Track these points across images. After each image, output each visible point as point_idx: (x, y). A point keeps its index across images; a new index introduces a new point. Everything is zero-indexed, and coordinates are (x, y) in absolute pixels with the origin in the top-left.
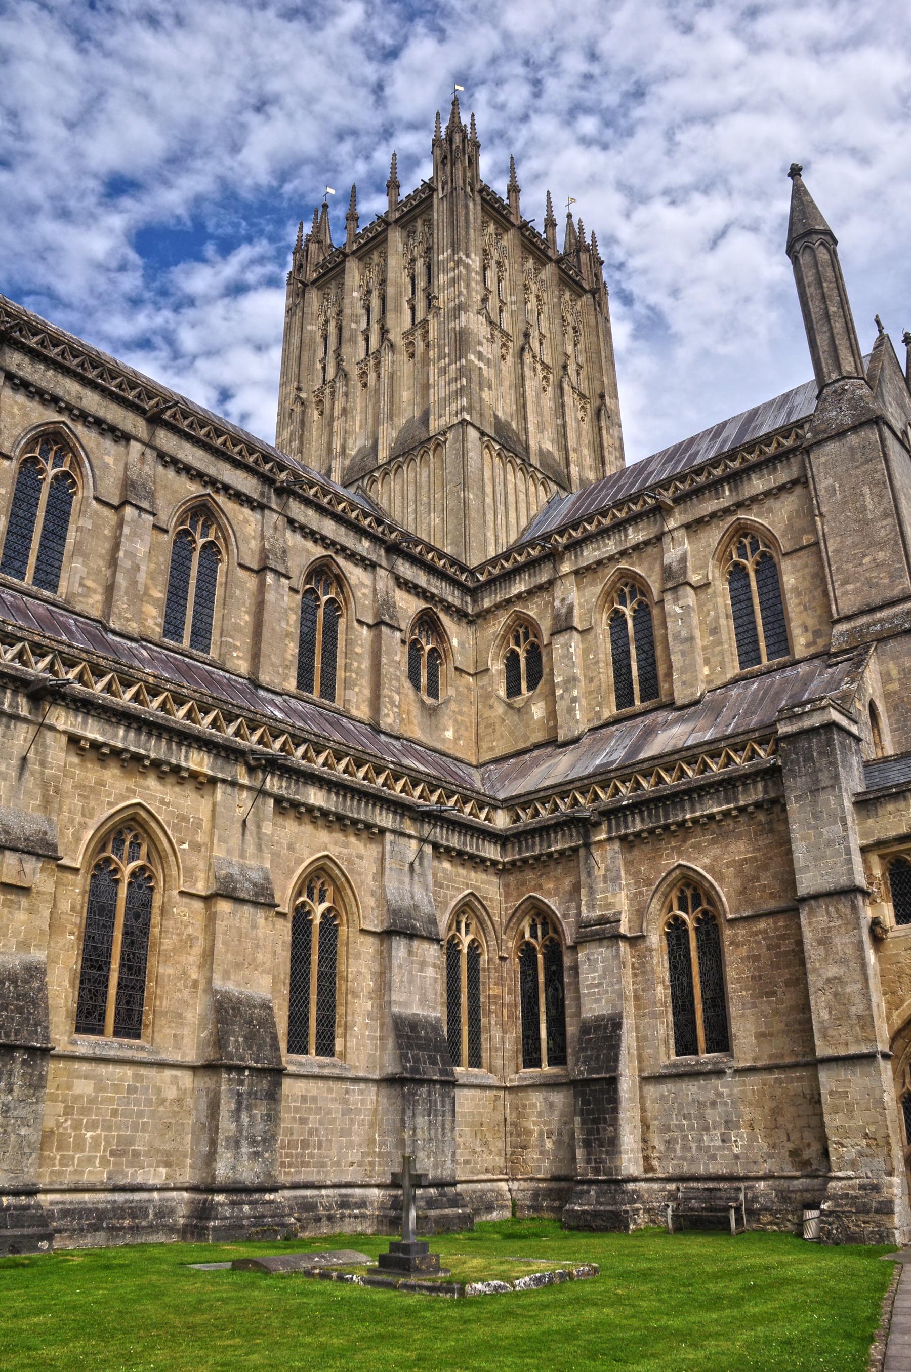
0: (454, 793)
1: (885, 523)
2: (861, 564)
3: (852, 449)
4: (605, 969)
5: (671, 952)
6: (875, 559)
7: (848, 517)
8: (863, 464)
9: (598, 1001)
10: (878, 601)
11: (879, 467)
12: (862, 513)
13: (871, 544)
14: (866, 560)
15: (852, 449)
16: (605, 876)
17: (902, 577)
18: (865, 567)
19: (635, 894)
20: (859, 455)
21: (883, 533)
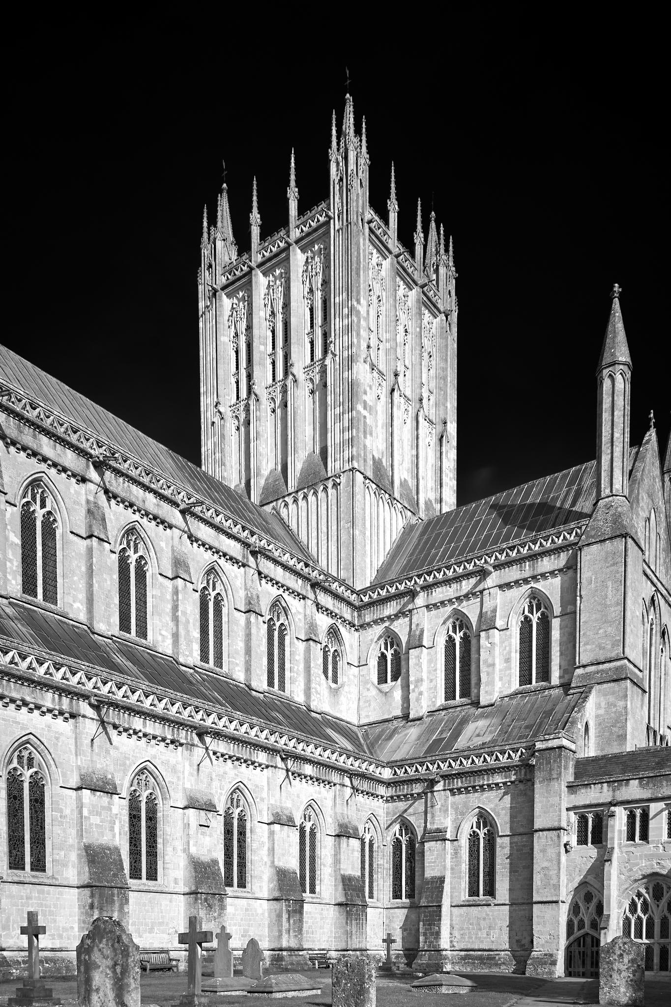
0: (365, 761)
1: (616, 609)
2: (597, 633)
3: (607, 553)
4: (437, 855)
5: (470, 848)
6: (606, 632)
7: (595, 601)
8: (613, 565)
9: (433, 870)
10: (602, 659)
11: (620, 570)
12: (604, 599)
13: (605, 622)
14: (601, 631)
15: (607, 553)
16: (440, 809)
17: (618, 646)
18: (599, 636)
19: (455, 819)
20: (611, 558)
21: (613, 615)
